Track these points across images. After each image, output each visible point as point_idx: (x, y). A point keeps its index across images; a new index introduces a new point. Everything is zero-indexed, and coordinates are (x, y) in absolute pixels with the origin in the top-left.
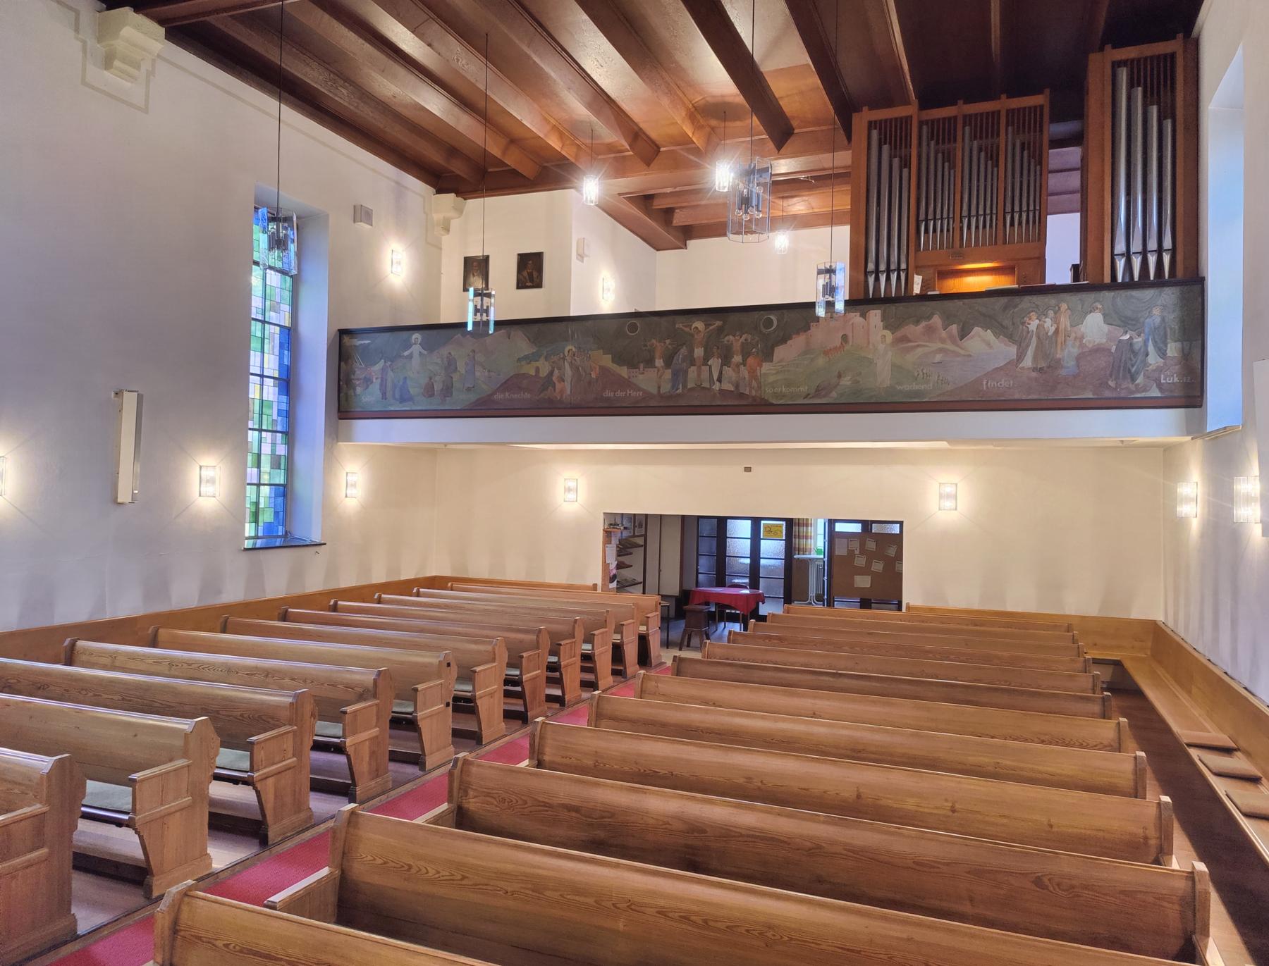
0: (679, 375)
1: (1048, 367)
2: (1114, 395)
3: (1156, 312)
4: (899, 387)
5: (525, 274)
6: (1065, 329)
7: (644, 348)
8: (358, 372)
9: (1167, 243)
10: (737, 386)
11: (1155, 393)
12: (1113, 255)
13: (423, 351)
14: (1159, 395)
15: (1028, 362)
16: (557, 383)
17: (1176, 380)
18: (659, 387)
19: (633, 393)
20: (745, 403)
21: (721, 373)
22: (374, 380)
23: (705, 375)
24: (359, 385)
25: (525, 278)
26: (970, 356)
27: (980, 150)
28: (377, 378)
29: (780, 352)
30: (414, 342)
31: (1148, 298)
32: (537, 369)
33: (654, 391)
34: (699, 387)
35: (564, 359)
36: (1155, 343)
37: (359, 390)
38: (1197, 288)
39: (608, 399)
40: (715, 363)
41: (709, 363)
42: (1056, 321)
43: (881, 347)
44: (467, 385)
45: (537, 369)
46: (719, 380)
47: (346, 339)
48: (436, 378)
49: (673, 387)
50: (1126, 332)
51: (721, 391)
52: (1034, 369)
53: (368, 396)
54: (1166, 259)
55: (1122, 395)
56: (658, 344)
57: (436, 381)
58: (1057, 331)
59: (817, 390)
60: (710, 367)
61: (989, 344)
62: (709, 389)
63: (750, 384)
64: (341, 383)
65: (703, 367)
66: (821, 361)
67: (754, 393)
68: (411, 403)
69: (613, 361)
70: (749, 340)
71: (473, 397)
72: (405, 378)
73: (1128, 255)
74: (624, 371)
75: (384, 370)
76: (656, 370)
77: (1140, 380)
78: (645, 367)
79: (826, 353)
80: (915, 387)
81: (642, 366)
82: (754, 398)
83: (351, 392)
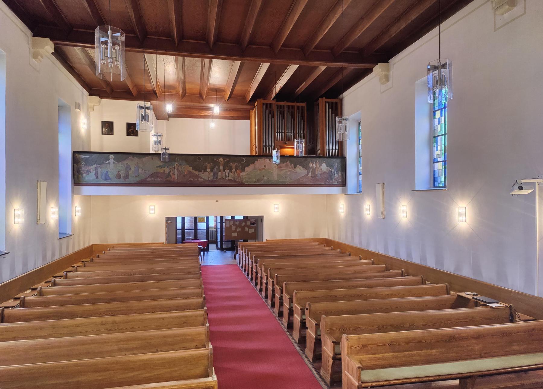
0: (215, 175)
1: (315, 176)
2: (328, 184)
3: (336, 164)
4: (279, 180)
5: (130, 130)
6: (318, 167)
7: (203, 165)
8: (83, 168)
9: (337, 148)
10: (234, 179)
11: (336, 183)
12: (326, 149)
13: (115, 162)
14: (337, 184)
15: (310, 175)
16: (172, 175)
17: (340, 181)
18: (209, 178)
19: (200, 180)
20: (237, 184)
21: (229, 174)
22: (92, 172)
23: (224, 175)
24: (83, 173)
25: (130, 132)
26: (296, 173)
27: (288, 112)
28: (93, 171)
29: (247, 169)
30: (110, 158)
31: (335, 160)
32: (164, 171)
33: (207, 179)
34: (222, 178)
35: (174, 167)
36: (336, 172)
37: (84, 175)
38: (344, 159)
39: (191, 181)
40: (227, 171)
41: (225, 171)
42: (316, 165)
43: (275, 169)
44: (135, 175)
45: (164, 171)
46: (228, 176)
47: (77, 155)
48: (121, 172)
49: (213, 178)
50: (330, 169)
51: (229, 179)
52: (311, 177)
53: (90, 177)
54: (337, 151)
55: (330, 184)
56: (208, 164)
57: (121, 173)
58: (316, 167)
59: (257, 180)
60: (225, 172)
61: (301, 170)
62: (225, 179)
63: (238, 178)
64: (75, 172)
65: (223, 172)
66: (258, 172)
67: (239, 181)
68: (110, 180)
69: (192, 169)
70: (237, 165)
71: (138, 179)
72: (107, 171)
73: (329, 149)
74: (197, 173)
75: (96, 168)
76: (208, 172)
77: (333, 180)
78: (204, 171)
79: (260, 170)
80: (284, 180)
81: (203, 171)
82: (239, 182)
83: (81, 176)
